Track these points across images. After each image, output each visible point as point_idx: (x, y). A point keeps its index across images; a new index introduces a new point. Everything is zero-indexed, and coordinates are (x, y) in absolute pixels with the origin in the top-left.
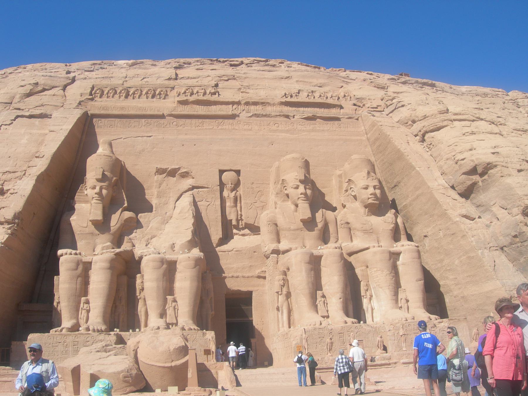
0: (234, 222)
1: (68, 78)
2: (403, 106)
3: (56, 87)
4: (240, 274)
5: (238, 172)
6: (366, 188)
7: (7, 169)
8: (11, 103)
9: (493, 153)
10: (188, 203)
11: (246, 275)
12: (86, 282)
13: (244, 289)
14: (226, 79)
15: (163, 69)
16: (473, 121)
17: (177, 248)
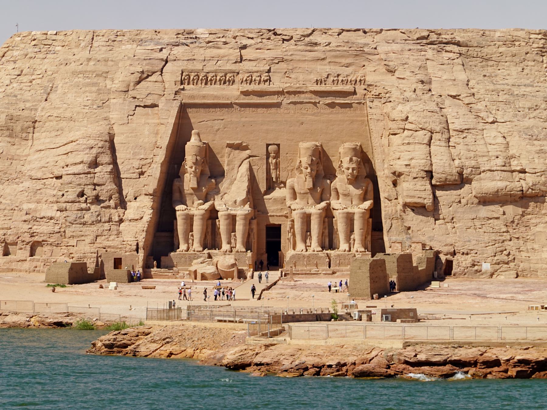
0: (274, 180)
1: (162, 60)
2: (390, 101)
3: (156, 72)
4: (275, 214)
5: (278, 145)
6: (348, 169)
7: (142, 157)
8: (128, 91)
9: (406, 165)
10: (245, 170)
11: (278, 214)
12: (192, 225)
13: (276, 223)
14: (277, 61)
15: (231, 51)
16: (416, 131)
17: (237, 203)
